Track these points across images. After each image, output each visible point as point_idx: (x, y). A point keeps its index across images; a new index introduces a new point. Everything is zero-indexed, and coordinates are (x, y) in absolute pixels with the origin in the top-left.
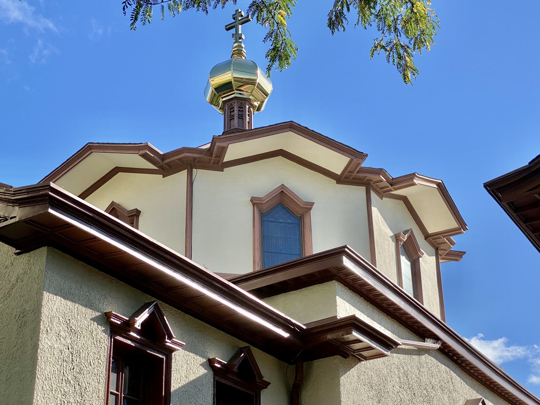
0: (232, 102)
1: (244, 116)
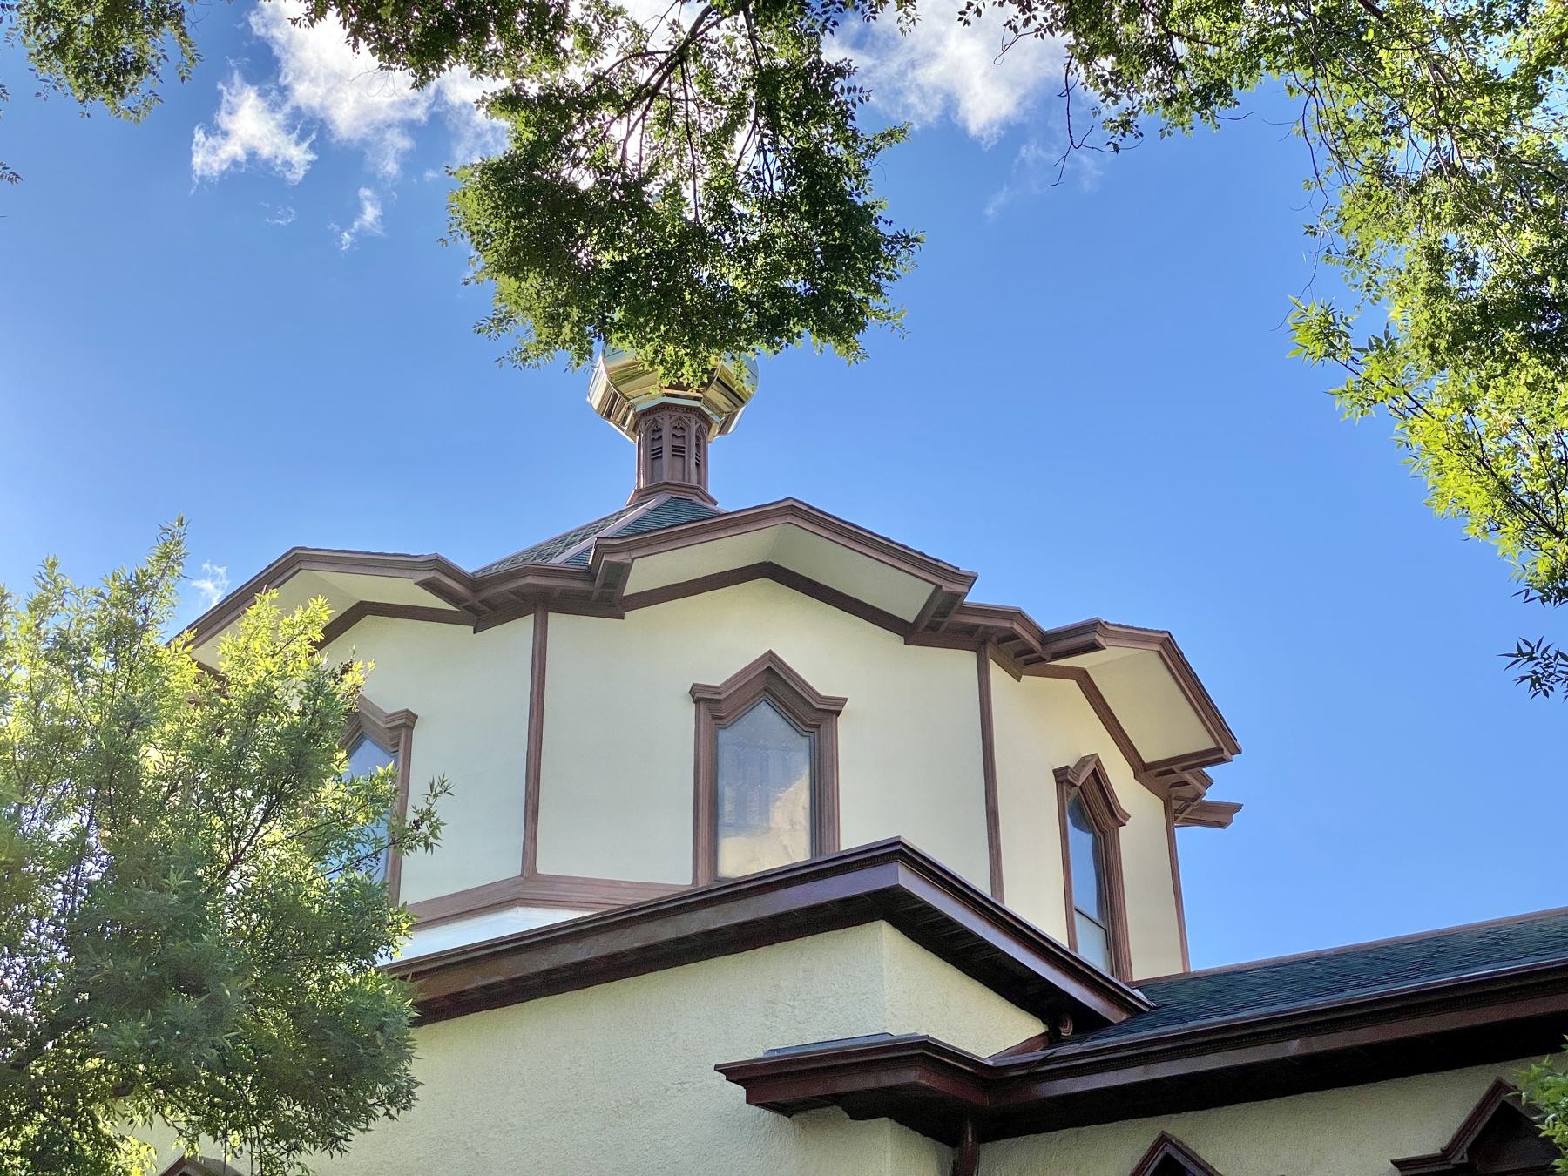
0: (656, 416)
1: (686, 450)
